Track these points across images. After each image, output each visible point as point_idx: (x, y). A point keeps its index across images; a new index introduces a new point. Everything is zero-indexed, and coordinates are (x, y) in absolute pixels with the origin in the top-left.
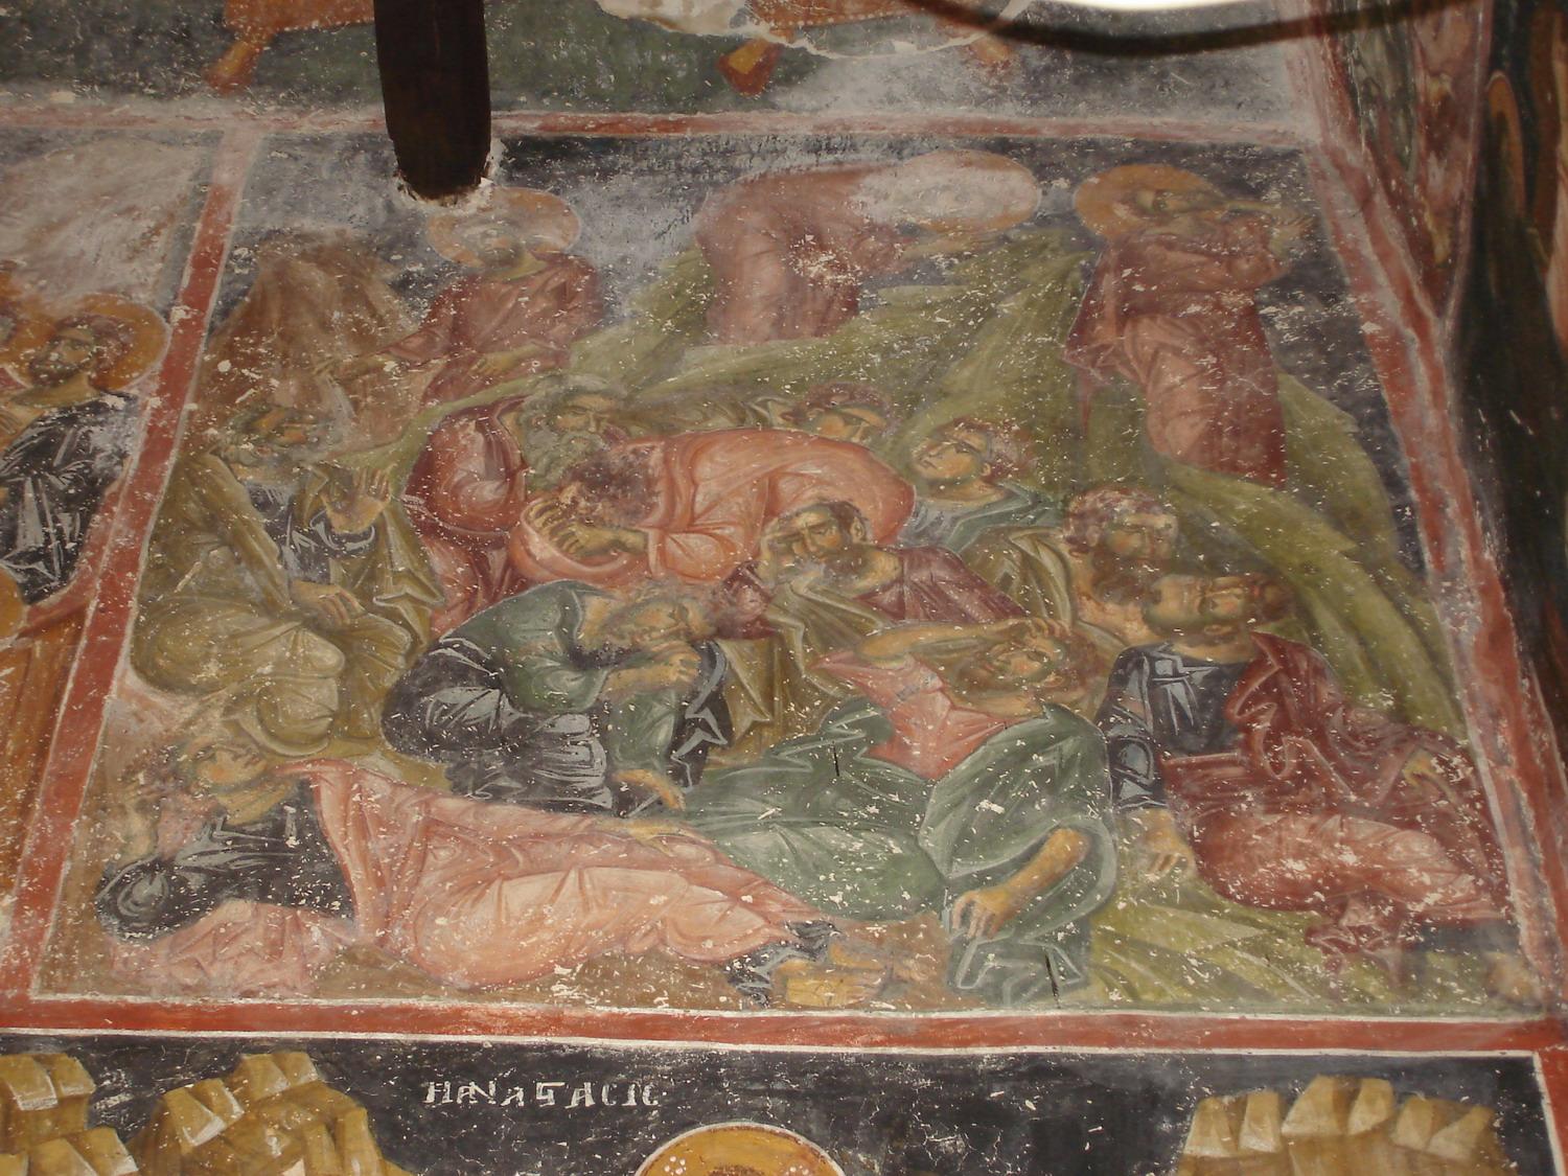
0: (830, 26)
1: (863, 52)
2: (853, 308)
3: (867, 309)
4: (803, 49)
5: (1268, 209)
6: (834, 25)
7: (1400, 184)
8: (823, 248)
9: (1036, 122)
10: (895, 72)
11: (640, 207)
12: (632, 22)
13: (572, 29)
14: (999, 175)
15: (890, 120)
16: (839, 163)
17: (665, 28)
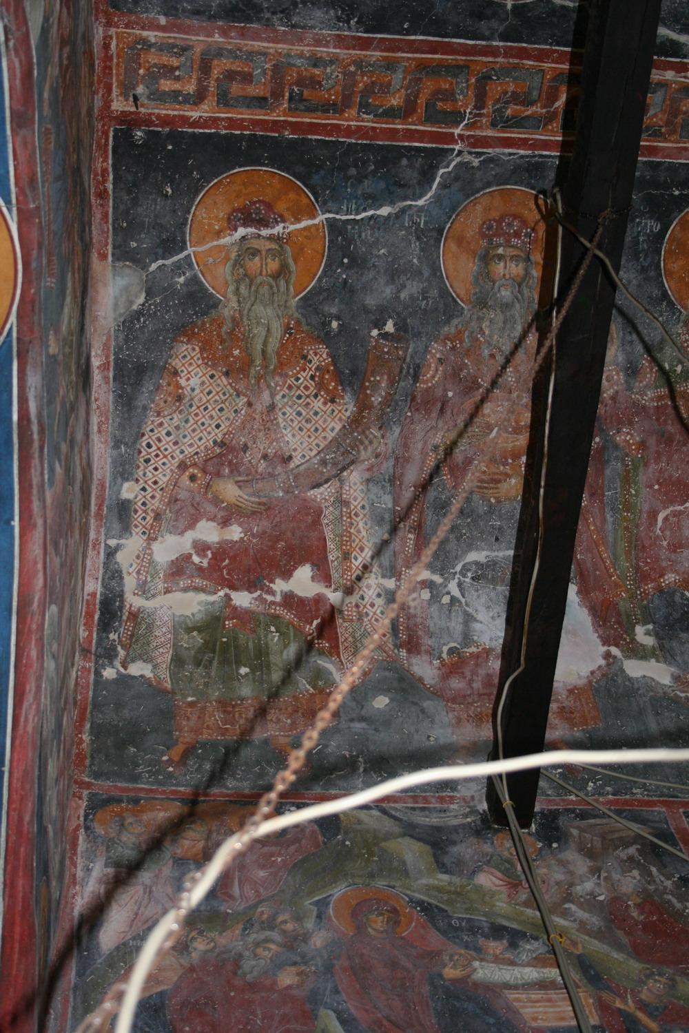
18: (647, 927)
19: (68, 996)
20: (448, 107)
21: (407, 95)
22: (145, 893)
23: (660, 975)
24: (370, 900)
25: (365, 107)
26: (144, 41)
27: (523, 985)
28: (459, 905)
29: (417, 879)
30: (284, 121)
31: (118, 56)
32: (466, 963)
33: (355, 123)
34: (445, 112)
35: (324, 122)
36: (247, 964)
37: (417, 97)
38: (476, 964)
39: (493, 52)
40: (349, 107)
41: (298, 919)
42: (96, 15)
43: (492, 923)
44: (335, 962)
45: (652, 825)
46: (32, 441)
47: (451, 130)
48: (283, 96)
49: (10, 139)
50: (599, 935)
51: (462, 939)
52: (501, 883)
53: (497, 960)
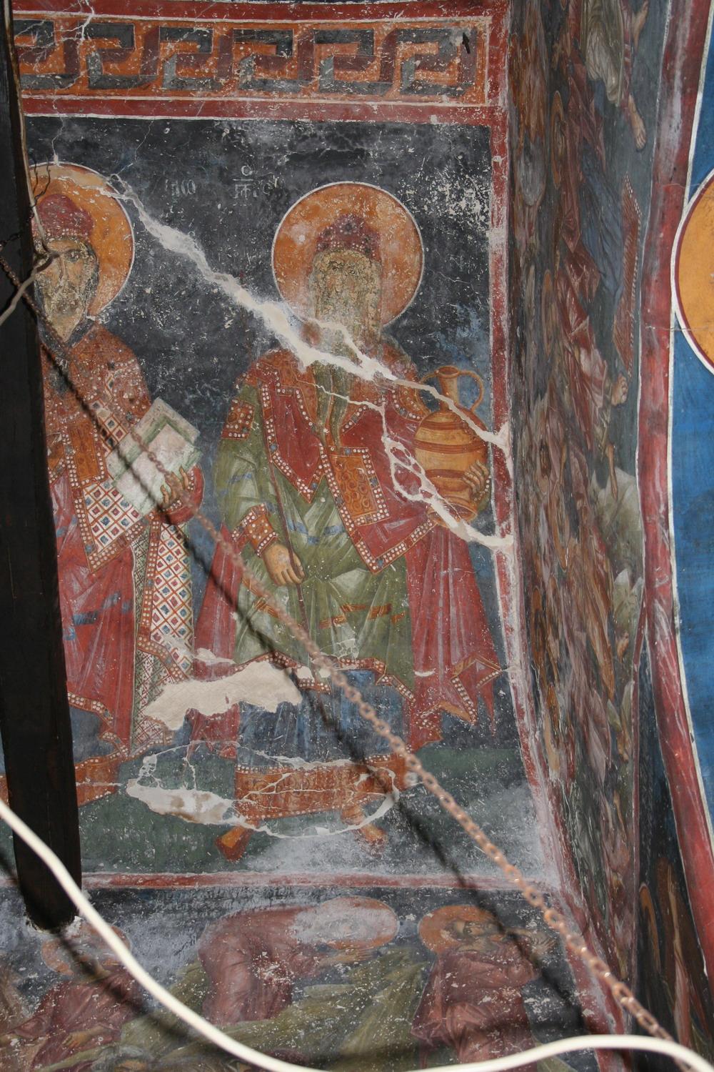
0: (280, 818)
1: (299, 834)
2: (289, 1000)
3: (297, 1000)
4: (264, 832)
5: (529, 934)
6: (283, 817)
7: (601, 925)
8: (272, 960)
9: (397, 877)
10: (317, 846)
11: (167, 934)
12: (167, 816)
13: (131, 821)
14: (375, 912)
15: (313, 877)
16: (283, 905)
17: (185, 820)
20: (107, 43)
21: (157, 54)
25: (205, 39)
26: (454, 95)
30: (297, 19)
31: (482, 76)
33: (214, 20)
34: (108, 36)
35: (251, 21)
37: (145, 52)
39: (63, 105)
40: (222, 38)
42: (505, 118)
46: (684, 69)
47: (100, 16)
48: (299, 46)
49: (670, 401)
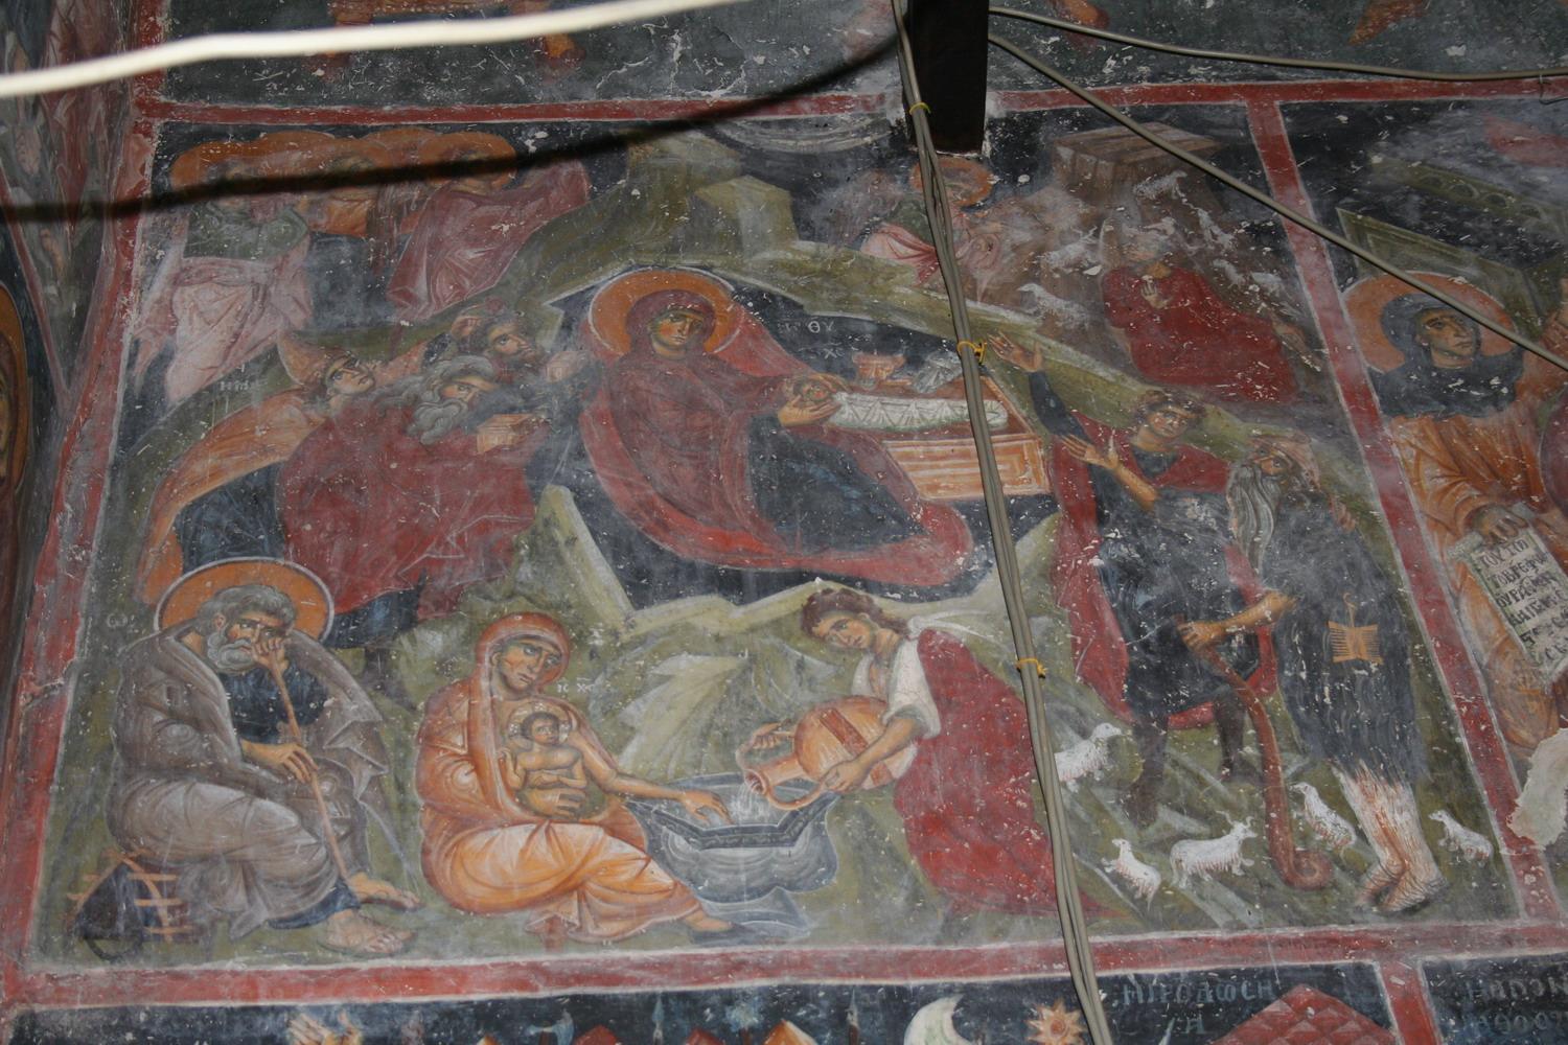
18: (1175, 321)
19: (102, 480)
22: (255, 298)
23: (1177, 403)
24: (666, 292)
27: (921, 431)
28: (825, 295)
29: (755, 252)
32: (822, 396)
36: (424, 415)
38: (842, 397)
41: (528, 331)
43: (881, 325)
44: (585, 404)
45: (1216, 132)
50: (1076, 338)
51: (823, 354)
52: (911, 252)
53: (882, 389)
